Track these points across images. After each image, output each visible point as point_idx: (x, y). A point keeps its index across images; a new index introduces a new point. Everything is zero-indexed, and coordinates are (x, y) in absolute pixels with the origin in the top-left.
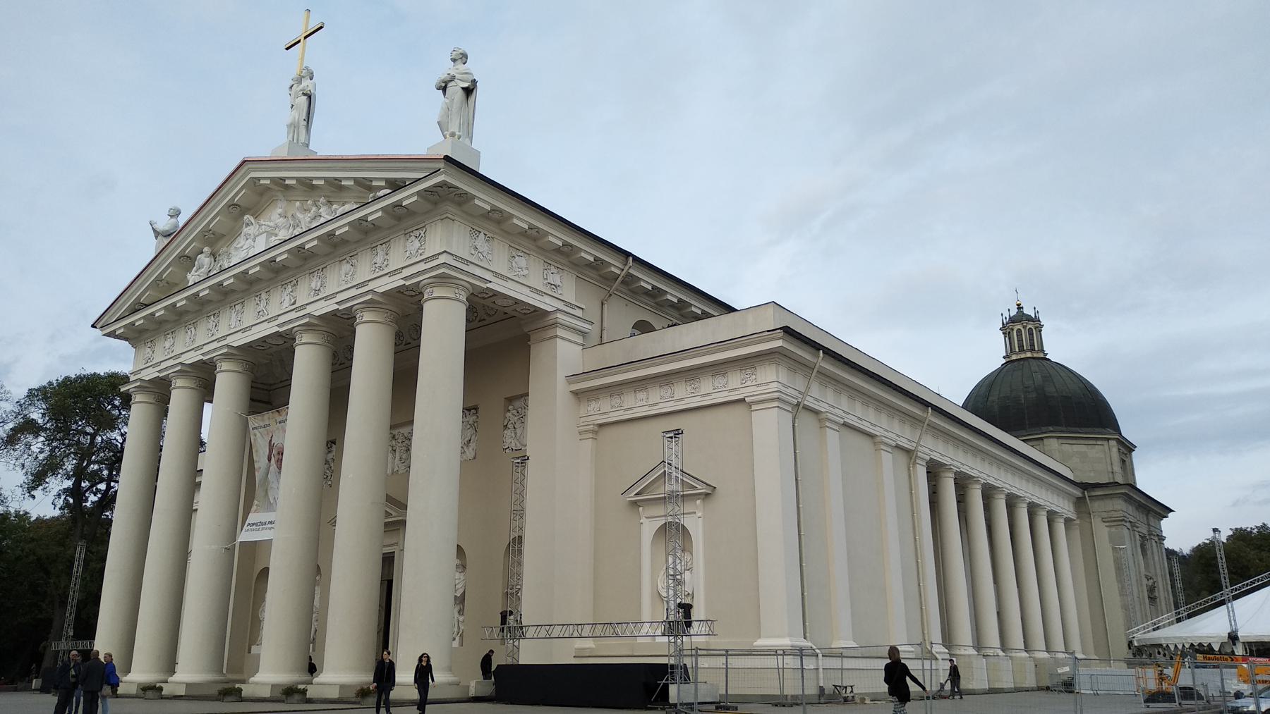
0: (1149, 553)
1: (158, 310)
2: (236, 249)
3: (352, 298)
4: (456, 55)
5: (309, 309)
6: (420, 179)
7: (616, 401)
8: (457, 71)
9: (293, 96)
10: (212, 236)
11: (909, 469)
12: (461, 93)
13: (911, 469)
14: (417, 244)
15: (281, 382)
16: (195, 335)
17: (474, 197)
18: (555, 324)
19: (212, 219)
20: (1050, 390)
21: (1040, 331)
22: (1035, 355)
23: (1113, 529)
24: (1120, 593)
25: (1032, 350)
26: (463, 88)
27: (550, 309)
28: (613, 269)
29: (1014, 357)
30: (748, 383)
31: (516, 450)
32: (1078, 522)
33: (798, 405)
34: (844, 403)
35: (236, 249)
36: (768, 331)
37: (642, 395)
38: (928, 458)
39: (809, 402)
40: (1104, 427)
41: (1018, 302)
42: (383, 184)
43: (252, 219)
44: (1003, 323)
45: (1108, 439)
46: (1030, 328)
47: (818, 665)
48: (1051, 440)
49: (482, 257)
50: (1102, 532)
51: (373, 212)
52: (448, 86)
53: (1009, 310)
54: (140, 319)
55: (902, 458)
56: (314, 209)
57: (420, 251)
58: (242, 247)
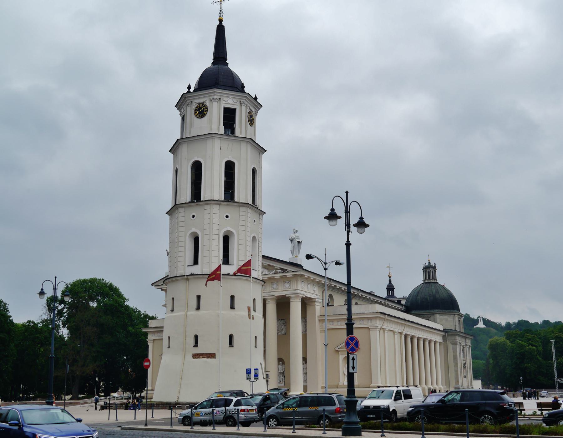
0: (465, 352)
12: (297, 243)
14: (288, 285)
17: (305, 275)
18: (315, 301)
20: (437, 296)
21: (436, 271)
22: (433, 281)
23: (454, 346)
27: (314, 297)
29: (426, 281)
30: (370, 323)
32: (443, 343)
37: (339, 323)
38: (405, 334)
40: (453, 309)
45: (455, 314)
46: (432, 271)
50: (450, 346)
51: (277, 276)
52: (294, 240)
55: (399, 335)
57: (289, 287)
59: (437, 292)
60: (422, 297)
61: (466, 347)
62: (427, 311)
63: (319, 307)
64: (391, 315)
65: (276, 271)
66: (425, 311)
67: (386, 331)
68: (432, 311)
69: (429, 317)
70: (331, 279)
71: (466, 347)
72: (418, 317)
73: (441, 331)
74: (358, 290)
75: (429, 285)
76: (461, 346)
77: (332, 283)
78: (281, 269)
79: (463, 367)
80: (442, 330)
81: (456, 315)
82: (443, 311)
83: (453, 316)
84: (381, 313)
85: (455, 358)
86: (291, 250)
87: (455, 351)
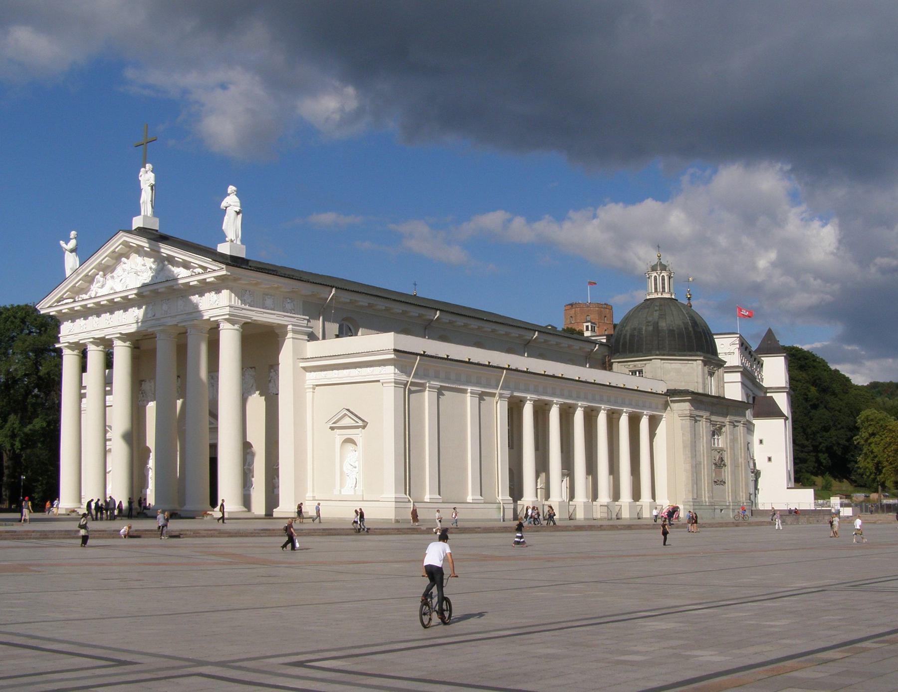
1: (77, 306)
20: (663, 325)
23: (684, 421)
25: (664, 291)
26: (236, 212)
46: (663, 276)
60: (632, 327)
69: (643, 367)
78: (201, 267)
80: (665, 391)
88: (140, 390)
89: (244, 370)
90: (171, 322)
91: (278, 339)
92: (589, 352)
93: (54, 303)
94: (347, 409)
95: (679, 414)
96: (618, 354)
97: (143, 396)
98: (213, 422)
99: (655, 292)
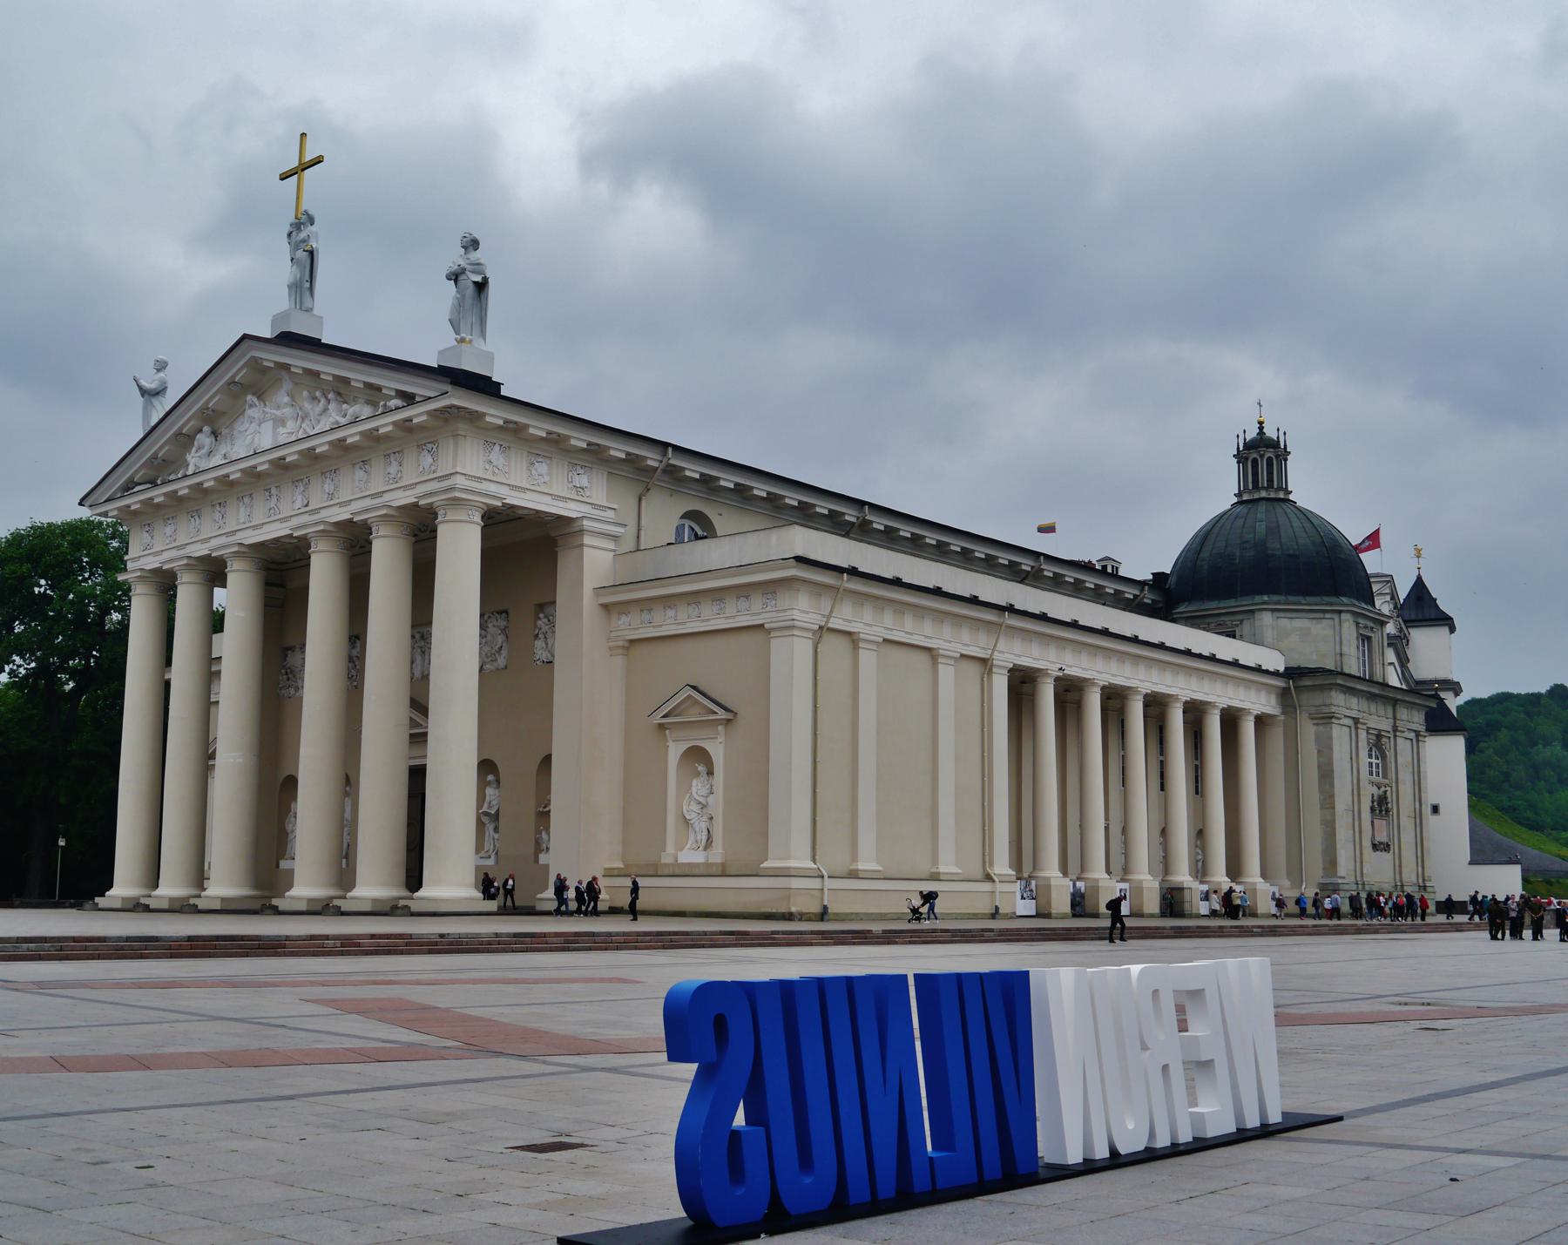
0: (1390, 754)
2: (240, 432)
3: (367, 510)
4: (467, 242)
5: (323, 514)
6: (430, 398)
7: (646, 616)
8: (468, 262)
9: (293, 244)
10: (211, 413)
11: (982, 680)
12: (471, 289)
13: (985, 679)
14: (427, 460)
15: (295, 561)
16: (200, 524)
17: (484, 415)
18: (581, 532)
19: (211, 396)
20: (1273, 546)
21: (1286, 460)
22: (1272, 495)
23: (1321, 728)
24: (1321, 804)
25: (1270, 485)
26: (475, 283)
27: (574, 515)
28: (650, 463)
29: (1245, 497)
30: (769, 609)
31: (548, 662)
32: (1282, 718)
33: (821, 628)
34: (888, 618)
35: (240, 432)
36: (783, 559)
37: (670, 613)
38: (1011, 666)
39: (834, 624)
40: (1337, 593)
41: (1262, 419)
42: (393, 394)
43: (255, 400)
44: (1238, 448)
45: (1340, 612)
47: (823, 885)
48: (1264, 613)
49: (497, 471)
50: (1308, 731)
51: (385, 424)
52: (461, 278)
53: (1245, 432)
54: (136, 503)
55: (973, 670)
56: (323, 401)
57: (433, 468)
58: (246, 431)
59: (1274, 530)
61: (1395, 736)
62: (1232, 602)
63: (612, 554)
64: (981, 598)
65: (385, 405)
66: (1223, 604)
67: (861, 645)
68: (1245, 603)
69: (1237, 626)
70: (666, 445)
71: (1395, 736)
72: (1192, 626)
73: (1276, 674)
74: (861, 504)
75: (1250, 509)
76: (1363, 735)
77: (671, 462)
78: (402, 395)
79: (1372, 809)
80: (1282, 669)
81: (1345, 616)
82: (1291, 598)
83: (1333, 619)
84: (801, 560)
85: (1326, 775)
86: (450, 320)
87: (1325, 749)
88: (284, 667)
89: (486, 617)
90: (342, 515)
91: (557, 549)
92: (1129, 599)
93: (115, 492)
94: (694, 688)
95: (1310, 714)
96: (1187, 603)
97: (288, 679)
98: (421, 722)
99: (1253, 488)
